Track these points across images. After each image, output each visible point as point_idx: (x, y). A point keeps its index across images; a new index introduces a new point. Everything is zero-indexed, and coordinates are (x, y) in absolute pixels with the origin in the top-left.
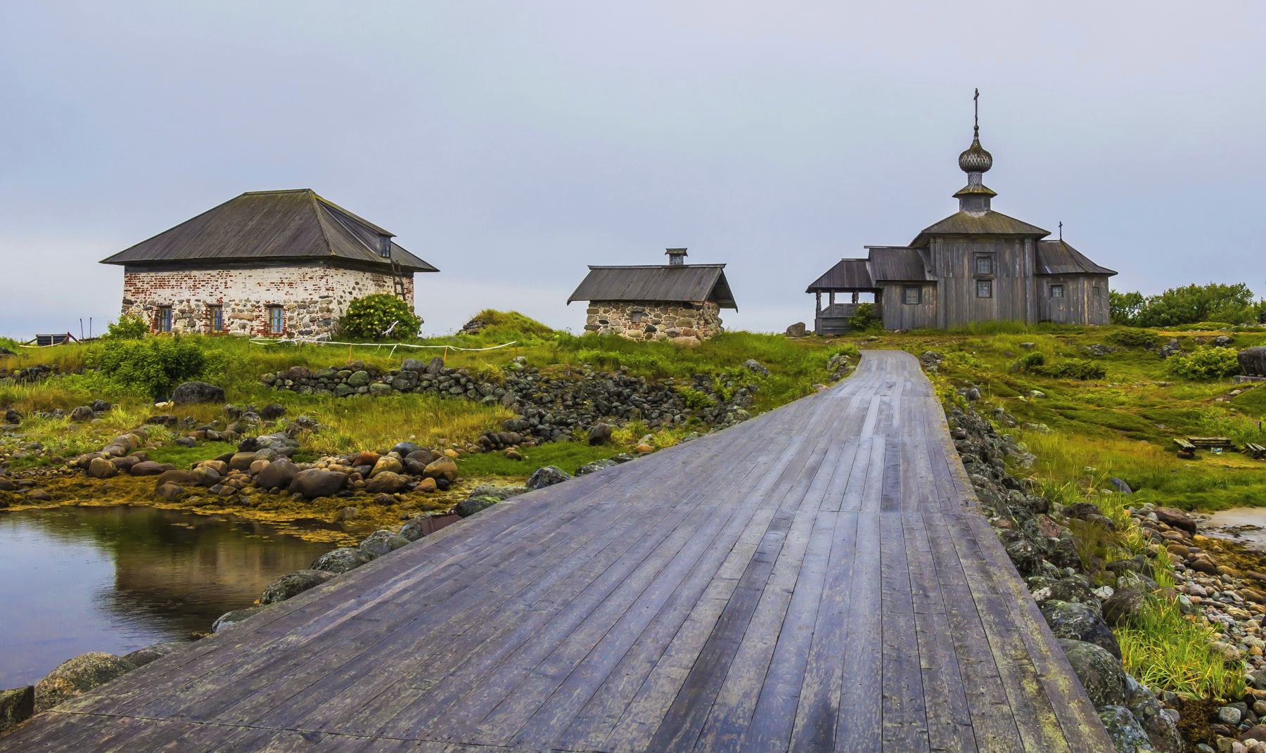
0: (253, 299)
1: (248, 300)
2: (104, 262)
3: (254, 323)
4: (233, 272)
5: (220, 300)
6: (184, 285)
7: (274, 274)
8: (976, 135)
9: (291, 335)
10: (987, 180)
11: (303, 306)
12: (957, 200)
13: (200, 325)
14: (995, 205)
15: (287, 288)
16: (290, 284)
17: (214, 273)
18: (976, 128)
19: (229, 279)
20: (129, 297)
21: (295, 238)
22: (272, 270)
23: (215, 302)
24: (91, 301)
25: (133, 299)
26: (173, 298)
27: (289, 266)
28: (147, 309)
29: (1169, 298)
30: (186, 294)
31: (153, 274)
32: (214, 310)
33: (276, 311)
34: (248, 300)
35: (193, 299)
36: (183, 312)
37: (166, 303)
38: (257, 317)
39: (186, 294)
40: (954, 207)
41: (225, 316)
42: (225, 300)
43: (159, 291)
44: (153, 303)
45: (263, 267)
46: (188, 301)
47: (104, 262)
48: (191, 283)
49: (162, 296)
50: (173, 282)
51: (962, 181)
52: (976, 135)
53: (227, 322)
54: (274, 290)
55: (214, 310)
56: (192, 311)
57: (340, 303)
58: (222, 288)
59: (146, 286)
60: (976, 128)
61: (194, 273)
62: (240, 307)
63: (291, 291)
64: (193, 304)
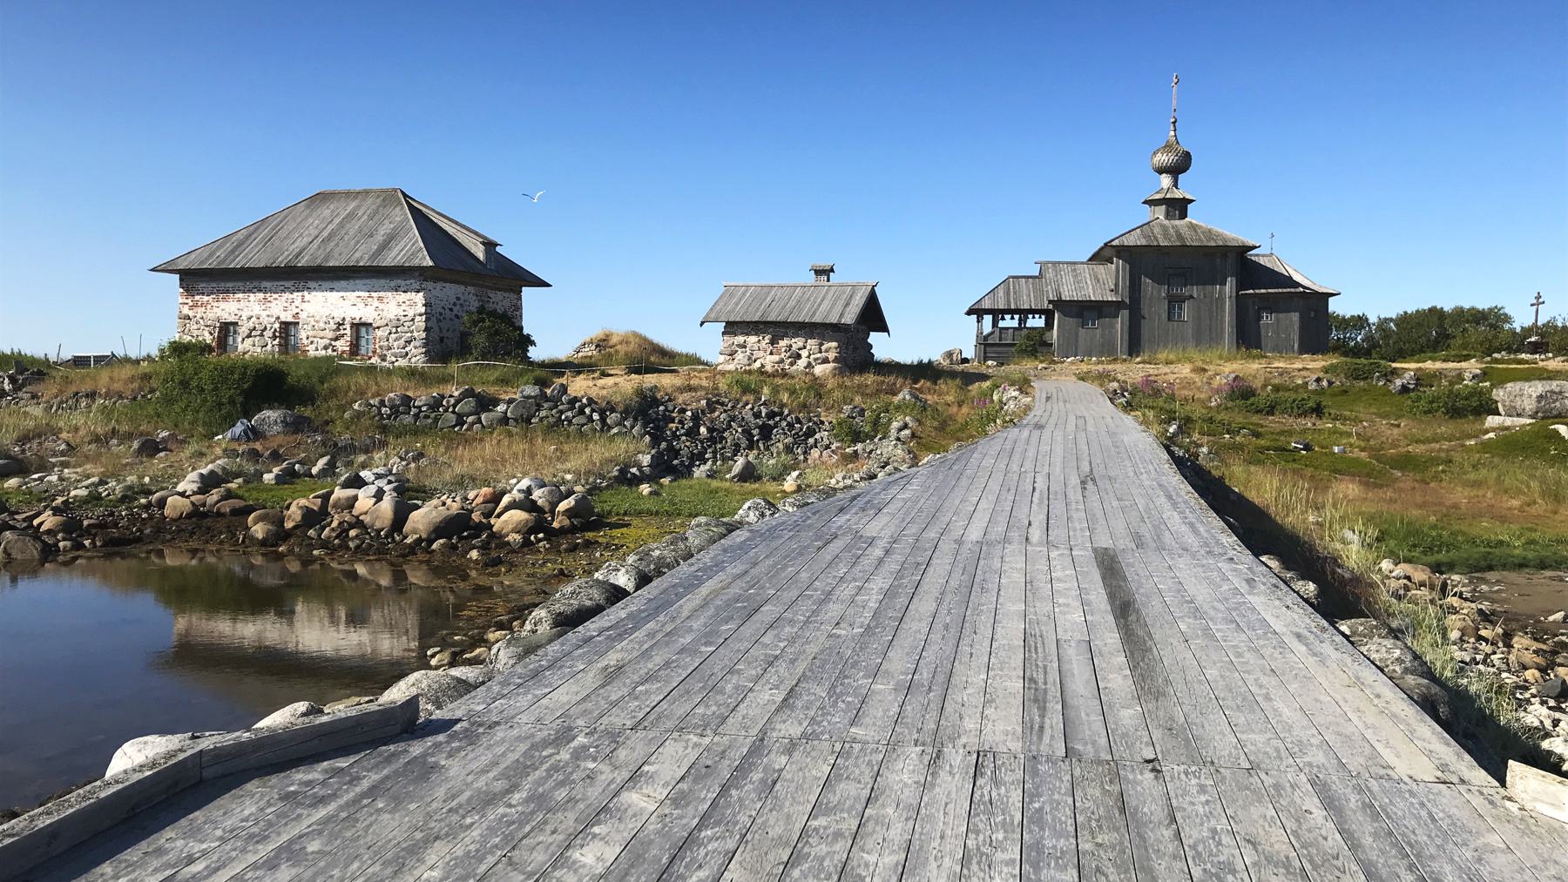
2: (153, 270)
3: (337, 343)
9: (383, 358)
11: (398, 324)
15: (376, 303)
20: (186, 310)
21: (385, 246)
23: (290, 319)
24: (142, 320)
25: (191, 314)
27: (378, 277)
29: (1404, 320)
32: (286, 330)
33: (363, 330)
35: (264, 314)
37: (232, 319)
42: (303, 316)
43: (223, 305)
45: (347, 278)
47: (153, 270)
48: (261, 295)
55: (286, 330)
57: (439, 321)
58: (298, 302)
62: (322, 325)
63: (381, 306)
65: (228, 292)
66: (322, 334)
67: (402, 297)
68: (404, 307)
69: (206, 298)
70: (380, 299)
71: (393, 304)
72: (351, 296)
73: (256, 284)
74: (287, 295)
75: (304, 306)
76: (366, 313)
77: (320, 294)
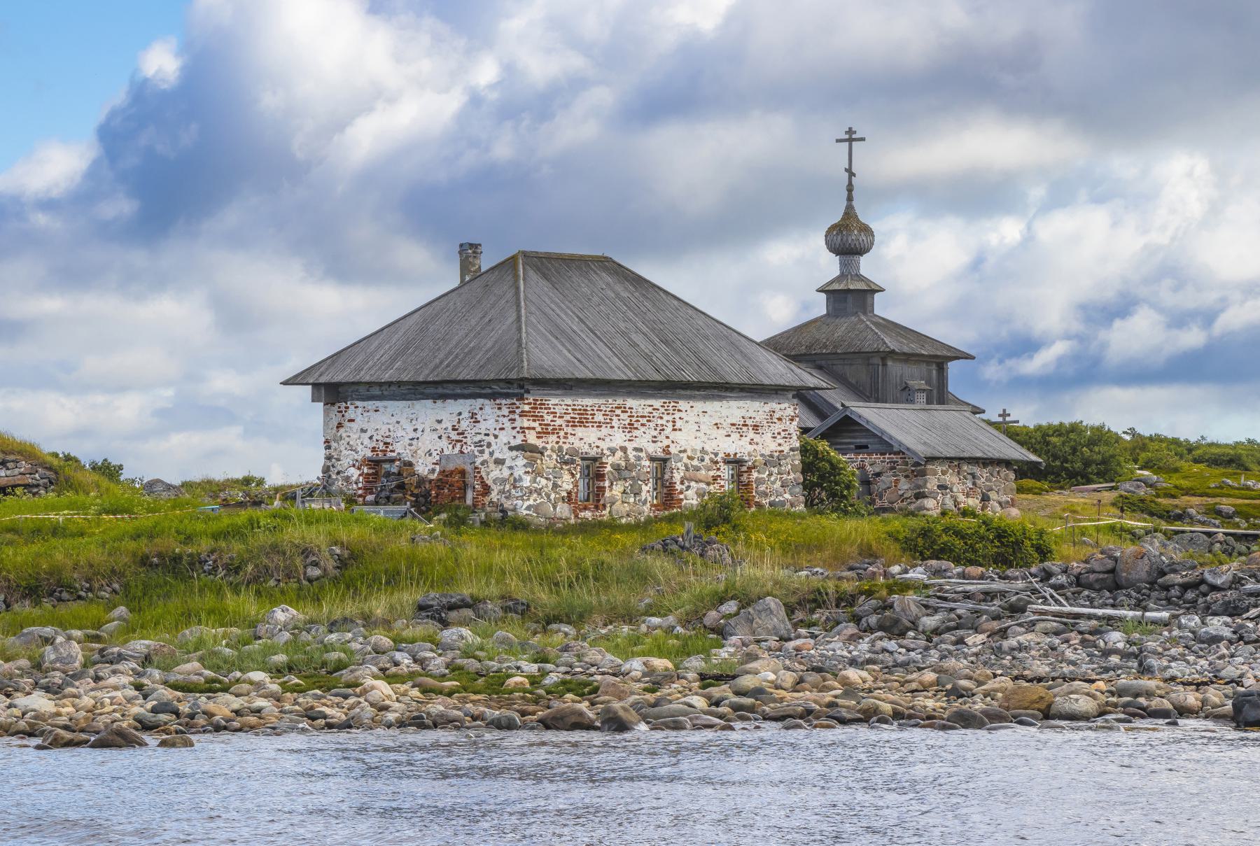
1: (703, 451)
4: (683, 404)
5: (666, 450)
6: (615, 423)
7: (734, 410)
8: (850, 199)
12: (823, 296)
15: (751, 434)
16: (756, 427)
17: (657, 403)
18: (850, 189)
19: (677, 415)
25: (539, 443)
28: (566, 463)
30: (619, 439)
34: (703, 451)
36: (617, 468)
39: (619, 439)
40: (820, 307)
42: (673, 450)
43: (580, 431)
44: (574, 452)
45: (721, 398)
46: (624, 449)
49: (586, 439)
50: (599, 417)
51: (830, 266)
52: (850, 199)
53: (678, 487)
56: (629, 467)
58: (668, 430)
59: (559, 422)
60: (850, 189)
61: (631, 402)
62: (695, 463)
63: (757, 438)
64: (631, 454)
73: (620, 401)
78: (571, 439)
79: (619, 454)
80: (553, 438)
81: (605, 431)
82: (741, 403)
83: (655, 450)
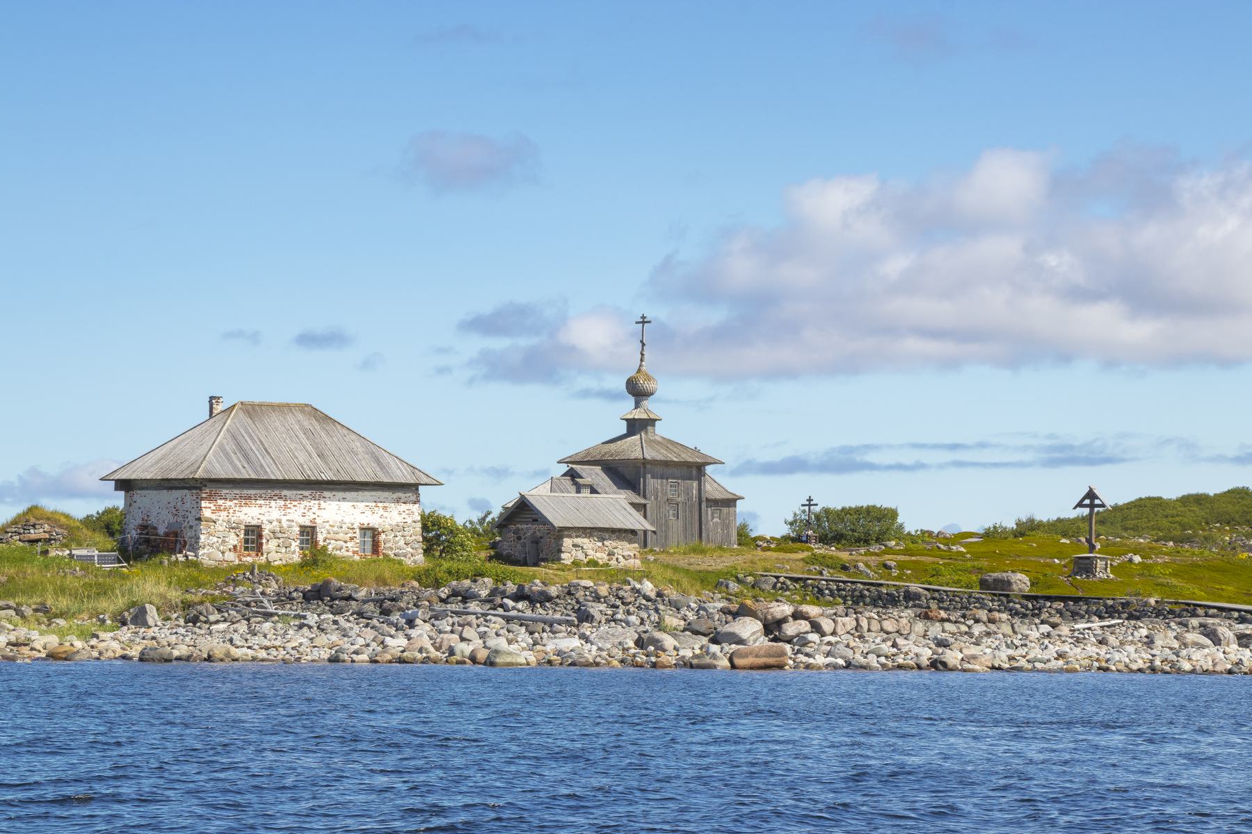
0: (348, 520)
1: (342, 522)
3: (349, 544)
10: (652, 407)
13: (295, 545)
14: (661, 430)
15: (381, 512)
17: (306, 493)
22: (367, 493)
25: (214, 517)
26: (262, 517)
27: (383, 490)
31: (237, 491)
34: (342, 522)
35: (284, 519)
37: (254, 522)
38: (352, 539)
41: (320, 538)
43: (245, 510)
45: (357, 490)
48: (282, 503)
54: (369, 513)
58: (315, 509)
63: (386, 514)
64: (285, 524)
65: (250, 498)
66: (337, 536)
67: (403, 507)
68: (404, 515)
69: (229, 503)
70: (385, 508)
71: (395, 513)
72: (361, 505)
73: (277, 492)
74: (305, 503)
75: (318, 513)
76: (373, 520)
77: (334, 504)
78: (238, 514)
79: (275, 523)
80: (225, 513)
81: (264, 509)
82: (374, 493)
83: (306, 522)
